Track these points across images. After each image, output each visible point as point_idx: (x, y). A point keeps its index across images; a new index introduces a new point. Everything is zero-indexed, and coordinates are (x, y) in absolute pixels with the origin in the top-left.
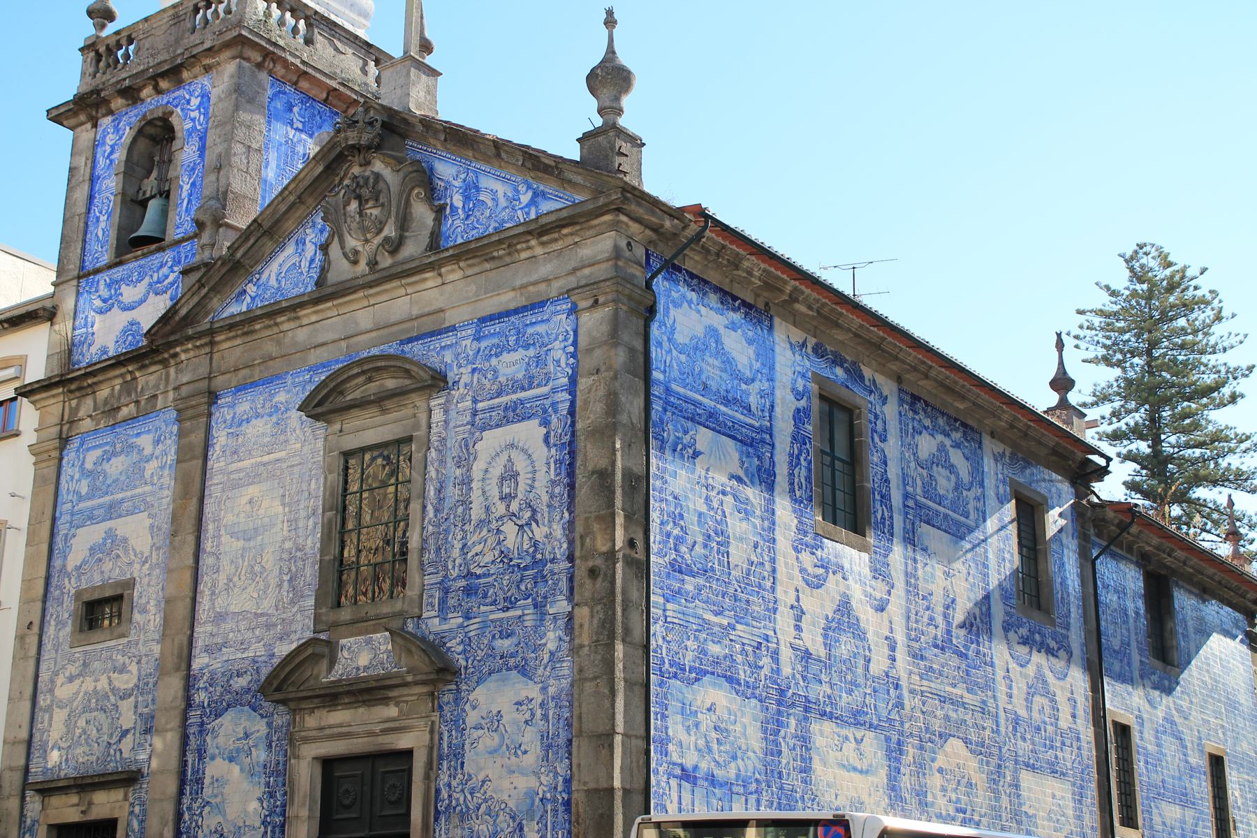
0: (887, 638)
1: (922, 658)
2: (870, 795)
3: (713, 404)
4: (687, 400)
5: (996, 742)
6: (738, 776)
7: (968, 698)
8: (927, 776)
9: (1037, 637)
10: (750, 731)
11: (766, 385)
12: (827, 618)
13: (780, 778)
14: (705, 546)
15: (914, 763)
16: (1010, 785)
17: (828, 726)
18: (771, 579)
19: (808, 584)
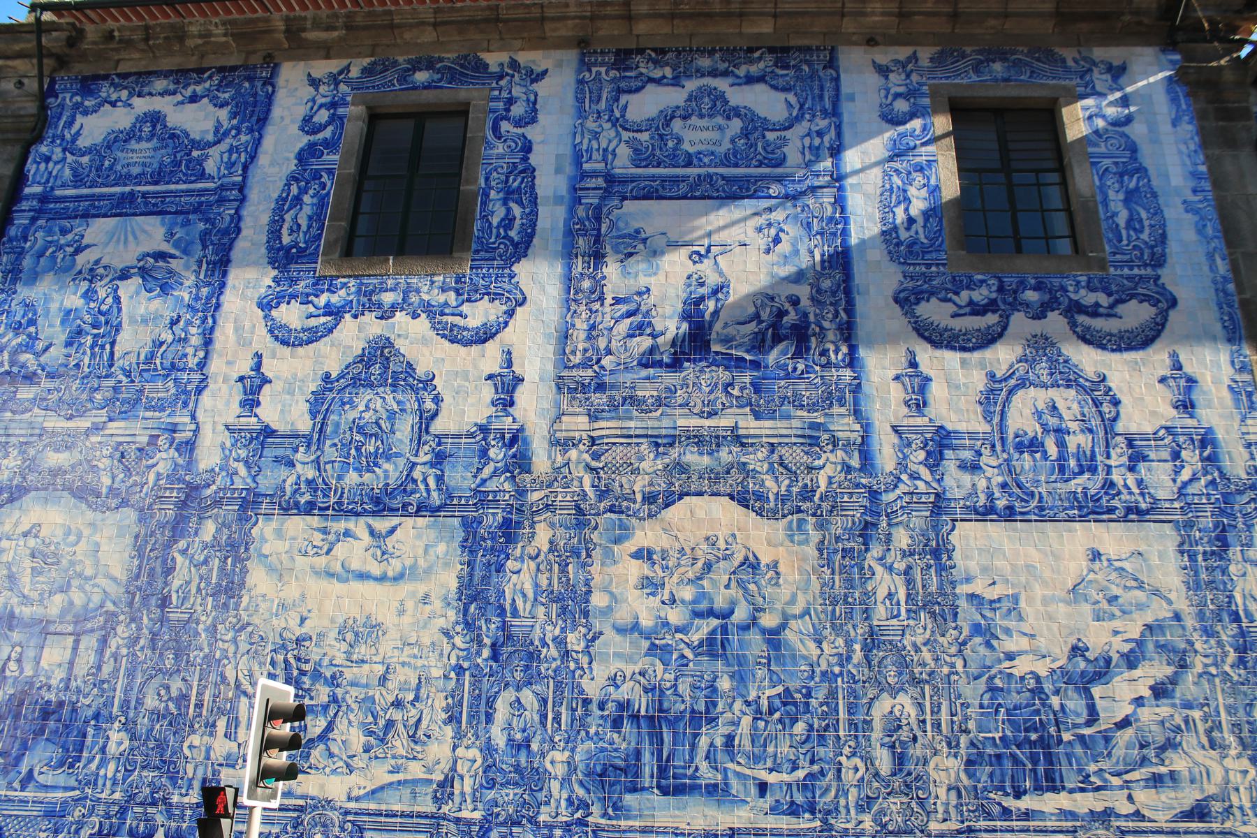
0: (490, 377)
1: (601, 387)
2: (401, 612)
3: (127, 189)
4: (78, 198)
5: (858, 485)
6: (64, 612)
7: (749, 425)
8: (595, 569)
9: (1031, 296)
10: (104, 548)
11: (244, 138)
12: (327, 377)
13: (164, 602)
14: (69, 344)
15: (550, 551)
16: (904, 554)
17: (298, 525)
18: (201, 354)
19: (285, 343)
